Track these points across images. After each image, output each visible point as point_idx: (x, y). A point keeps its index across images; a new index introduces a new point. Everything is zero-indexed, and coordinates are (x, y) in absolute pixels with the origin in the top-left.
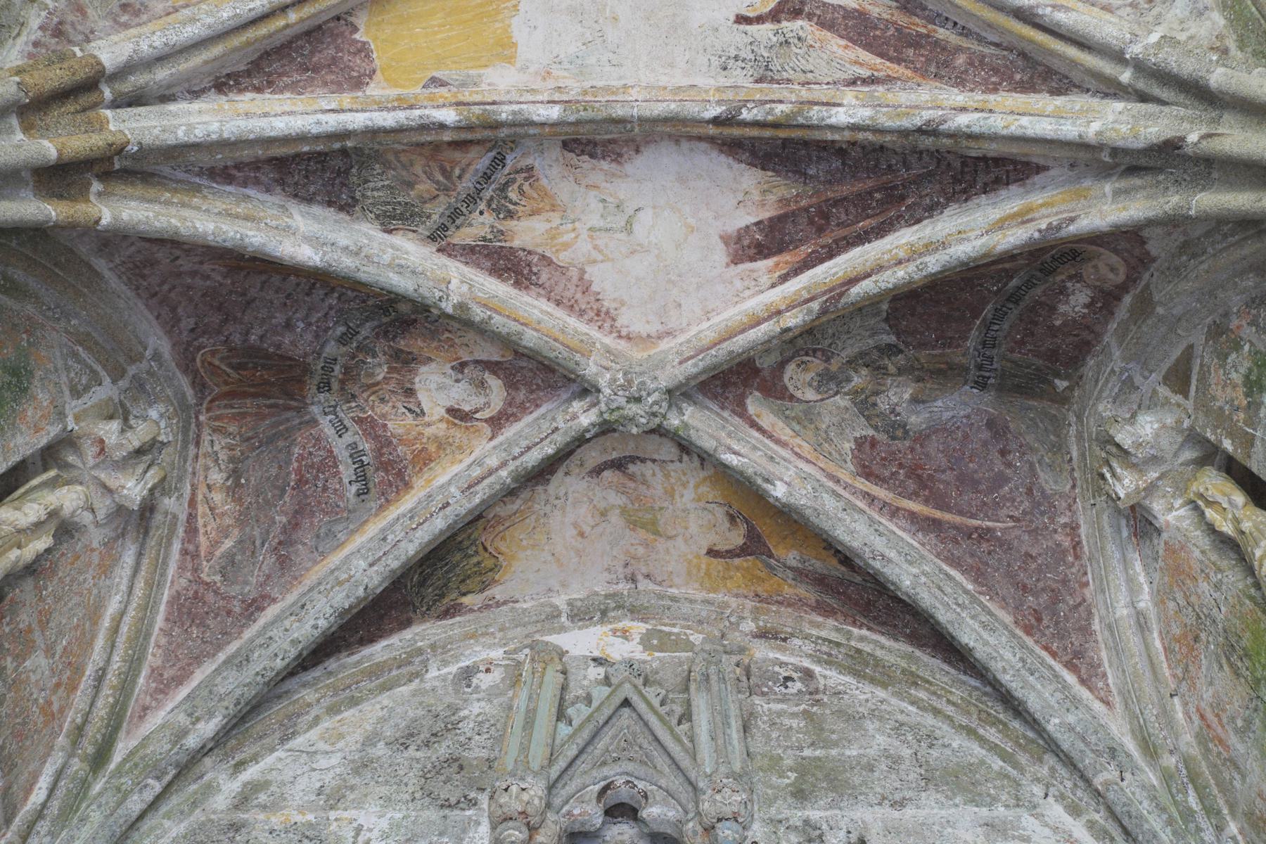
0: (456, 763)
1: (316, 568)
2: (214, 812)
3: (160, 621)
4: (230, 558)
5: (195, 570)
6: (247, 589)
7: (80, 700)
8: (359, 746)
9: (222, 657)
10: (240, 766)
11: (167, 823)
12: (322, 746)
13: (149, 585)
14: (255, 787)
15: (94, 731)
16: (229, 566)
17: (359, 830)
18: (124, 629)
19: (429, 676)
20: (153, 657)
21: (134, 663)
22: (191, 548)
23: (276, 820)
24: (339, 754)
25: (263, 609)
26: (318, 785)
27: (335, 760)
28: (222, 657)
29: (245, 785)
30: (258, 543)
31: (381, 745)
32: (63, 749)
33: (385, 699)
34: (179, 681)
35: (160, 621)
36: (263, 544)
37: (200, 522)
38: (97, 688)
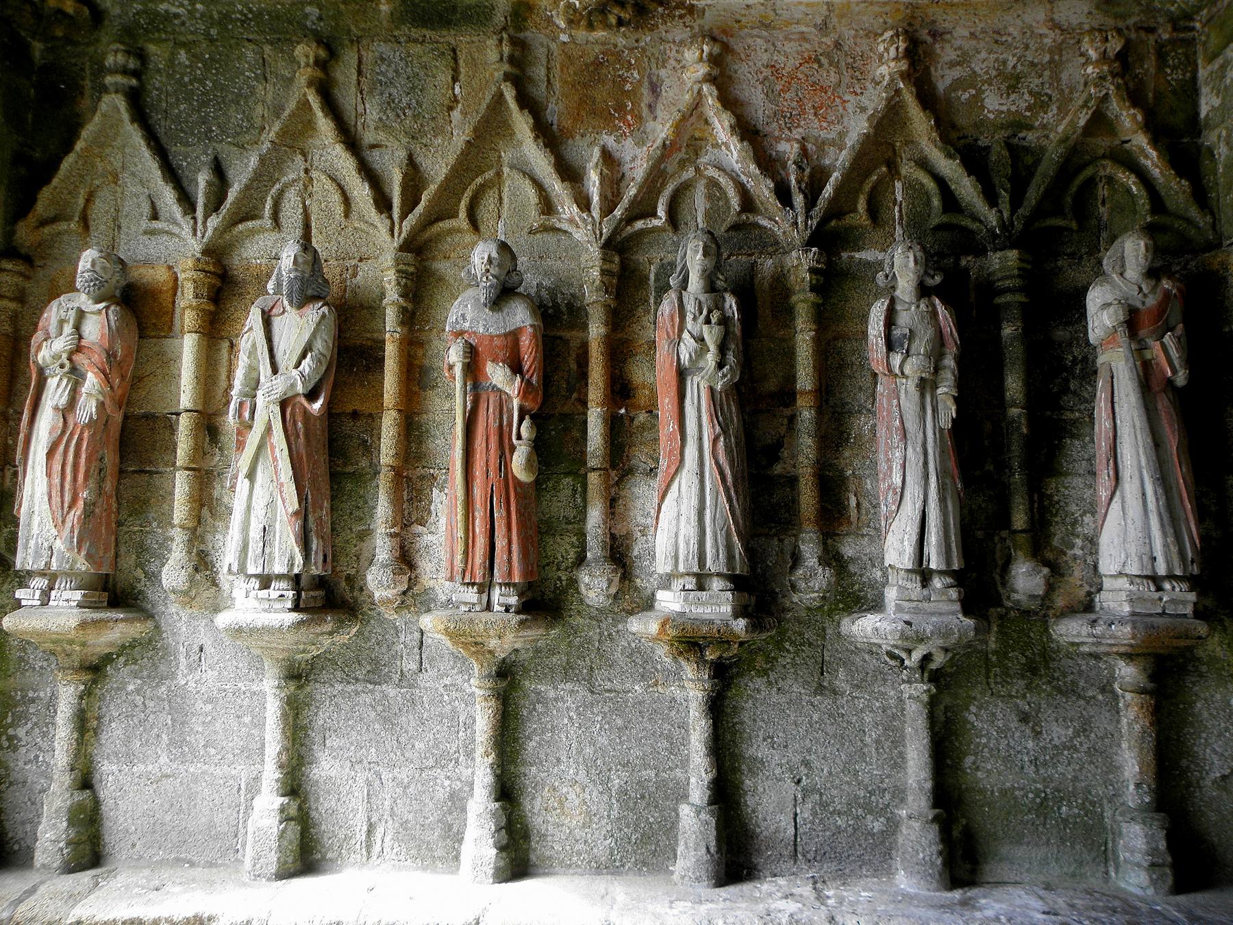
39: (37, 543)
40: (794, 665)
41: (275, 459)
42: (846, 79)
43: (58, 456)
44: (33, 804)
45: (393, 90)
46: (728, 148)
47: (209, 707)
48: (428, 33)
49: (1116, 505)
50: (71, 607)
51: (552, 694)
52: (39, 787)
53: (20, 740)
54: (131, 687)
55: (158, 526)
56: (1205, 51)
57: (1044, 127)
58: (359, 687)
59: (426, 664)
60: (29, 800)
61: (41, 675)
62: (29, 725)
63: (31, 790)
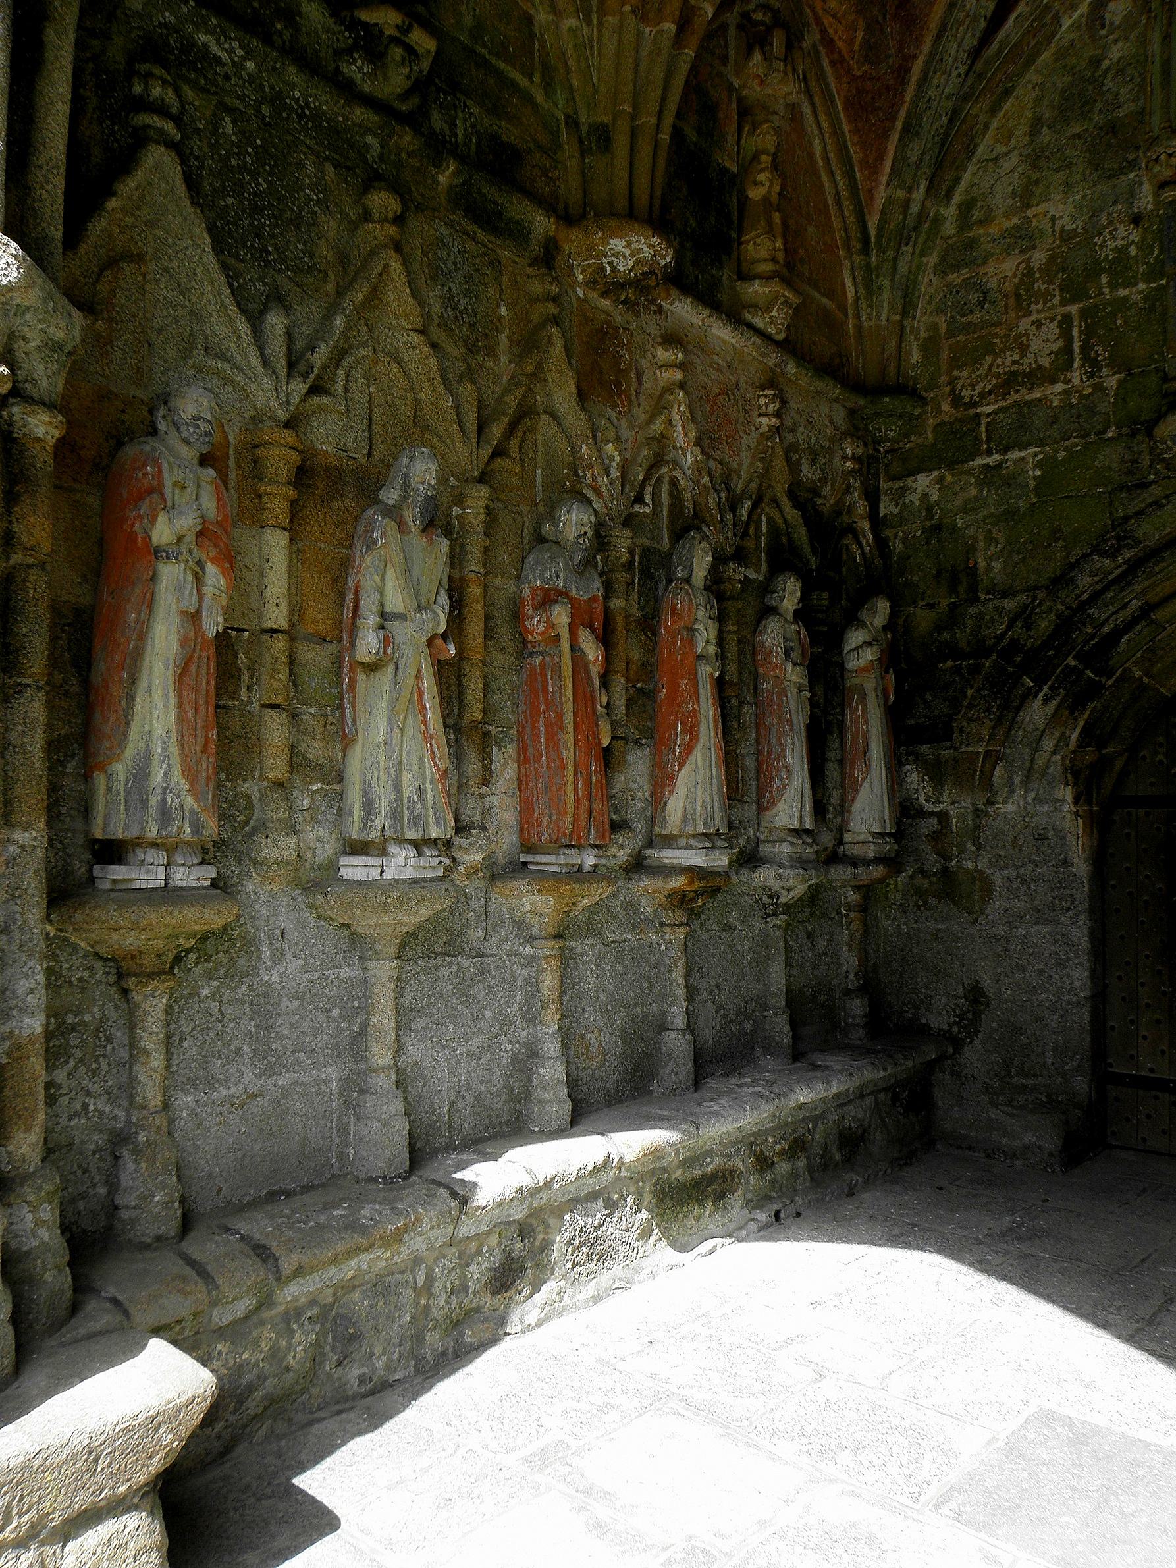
0: (1112, 128)
1: (936, 8)
2: (949, 238)
3: (846, 127)
4: (867, 45)
5: (848, 71)
6: (891, 61)
7: (836, 222)
8: (1027, 138)
9: (899, 124)
10: (949, 194)
11: (925, 260)
12: (1000, 149)
13: (829, 114)
14: (967, 206)
15: (855, 233)
16: (871, 53)
17: (1053, 219)
18: (832, 155)
19: (1064, 28)
20: (856, 154)
21: (850, 174)
22: (836, 56)
23: (994, 230)
24: (1015, 153)
25: (910, 69)
26: (1010, 189)
27: (1014, 159)
28: (899, 124)
29: (959, 206)
30: (880, 19)
31: (1045, 130)
32: (846, 258)
33: (1032, 76)
34: (880, 158)
35: (846, 127)
36: (885, 18)
37: (831, 32)
38: (841, 208)
39: (164, 800)
40: (713, 907)
41: (424, 707)
42: (742, 419)
43: (190, 681)
44: (85, 1171)
45: (452, 285)
46: (684, 453)
47: (296, 1003)
48: (480, 234)
49: (866, 784)
50: (205, 887)
51: (579, 950)
52: (92, 1147)
53: (59, 1087)
54: (206, 992)
55: (227, 779)
56: (887, 472)
57: (825, 497)
58: (439, 960)
59: (490, 932)
60: (79, 1166)
61: (83, 990)
62: (72, 1063)
63: (81, 1153)
